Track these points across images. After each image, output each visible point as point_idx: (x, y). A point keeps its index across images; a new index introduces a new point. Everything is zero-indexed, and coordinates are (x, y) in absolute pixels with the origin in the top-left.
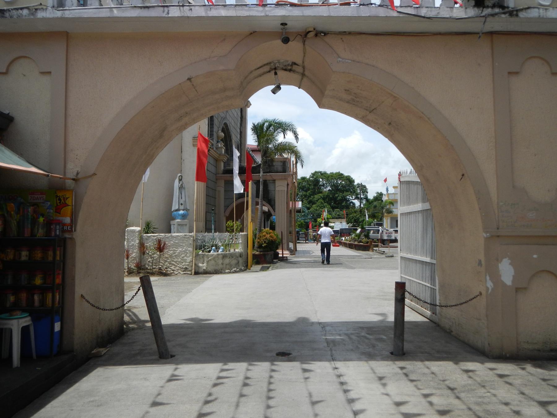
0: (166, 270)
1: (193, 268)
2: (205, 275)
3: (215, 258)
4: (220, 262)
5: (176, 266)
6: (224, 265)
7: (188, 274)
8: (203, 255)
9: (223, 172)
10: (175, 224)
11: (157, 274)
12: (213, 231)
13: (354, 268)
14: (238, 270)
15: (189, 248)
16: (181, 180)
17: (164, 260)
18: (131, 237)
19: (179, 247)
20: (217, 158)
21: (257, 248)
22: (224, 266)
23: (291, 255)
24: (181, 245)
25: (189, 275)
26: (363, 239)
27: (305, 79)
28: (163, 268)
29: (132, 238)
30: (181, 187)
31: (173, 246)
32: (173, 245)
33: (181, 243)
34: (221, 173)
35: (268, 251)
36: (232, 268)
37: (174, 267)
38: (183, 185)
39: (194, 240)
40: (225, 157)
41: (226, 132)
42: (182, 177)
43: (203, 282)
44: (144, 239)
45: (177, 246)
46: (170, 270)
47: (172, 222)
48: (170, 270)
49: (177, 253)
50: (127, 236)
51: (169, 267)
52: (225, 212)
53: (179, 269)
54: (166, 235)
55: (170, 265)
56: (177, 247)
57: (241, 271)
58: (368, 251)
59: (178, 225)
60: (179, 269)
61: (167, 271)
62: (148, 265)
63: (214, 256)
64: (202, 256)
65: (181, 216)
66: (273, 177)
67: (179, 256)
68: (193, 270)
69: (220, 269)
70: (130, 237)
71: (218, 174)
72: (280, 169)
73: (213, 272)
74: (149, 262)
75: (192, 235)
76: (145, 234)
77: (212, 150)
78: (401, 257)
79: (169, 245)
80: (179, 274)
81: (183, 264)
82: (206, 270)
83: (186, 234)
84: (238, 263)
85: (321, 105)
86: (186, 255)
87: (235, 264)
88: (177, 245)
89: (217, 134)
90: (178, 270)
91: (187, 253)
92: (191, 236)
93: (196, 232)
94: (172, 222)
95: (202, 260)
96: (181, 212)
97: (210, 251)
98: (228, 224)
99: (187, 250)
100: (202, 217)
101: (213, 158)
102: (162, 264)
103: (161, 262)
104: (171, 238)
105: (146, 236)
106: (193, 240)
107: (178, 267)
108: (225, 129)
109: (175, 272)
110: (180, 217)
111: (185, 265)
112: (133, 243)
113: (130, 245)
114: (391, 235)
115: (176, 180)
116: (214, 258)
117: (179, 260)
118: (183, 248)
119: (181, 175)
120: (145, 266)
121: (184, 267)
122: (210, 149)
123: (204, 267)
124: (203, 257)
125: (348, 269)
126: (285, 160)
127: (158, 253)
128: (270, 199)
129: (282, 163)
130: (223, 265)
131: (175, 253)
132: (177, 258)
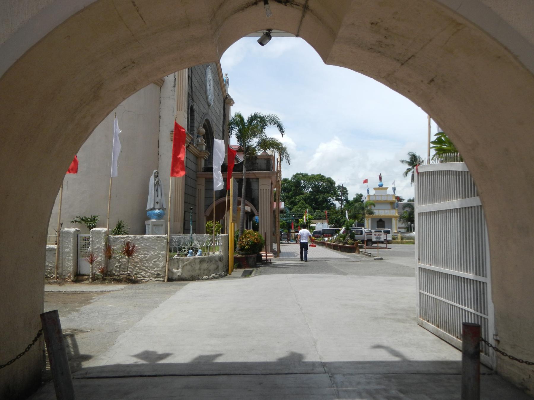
0: (135, 276)
1: (166, 274)
2: (179, 282)
3: (191, 263)
4: (197, 266)
5: (147, 272)
6: (202, 270)
7: (160, 281)
9: (204, 170)
10: (149, 225)
11: (125, 281)
12: (191, 232)
13: (345, 274)
14: (217, 275)
15: (162, 251)
16: (157, 176)
17: (134, 265)
18: (96, 239)
19: (150, 250)
20: (198, 156)
21: (238, 250)
22: (202, 271)
23: (274, 257)
24: (153, 248)
25: (161, 282)
26: (349, 240)
27: (308, 16)
28: (132, 274)
29: (97, 240)
30: (157, 184)
31: (143, 250)
32: (144, 248)
33: (153, 246)
34: (202, 170)
35: (250, 254)
36: (211, 273)
37: (144, 272)
38: (159, 181)
39: (168, 243)
40: (205, 154)
41: (208, 128)
42: (158, 173)
43: (176, 291)
44: (111, 241)
45: (148, 249)
46: (139, 276)
47: (147, 222)
48: (139, 276)
49: (148, 257)
50: (92, 237)
51: (139, 273)
52: (205, 212)
53: (151, 275)
54: (136, 237)
55: (141, 271)
56: (148, 250)
57: (221, 277)
58: (354, 252)
59: (153, 225)
60: (151, 275)
61: (137, 277)
62: (116, 271)
63: (190, 260)
64: (177, 260)
66: (257, 176)
67: (150, 261)
68: (166, 276)
69: (197, 275)
70: (95, 239)
71: (199, 172)
72: (264, 166)
73: (189, 279)
74: (117, 267)
75: (166, 237)
76: (113, 236)
77: (192, 146)
78: (419, 268)
79: (140, 248)
80: (150, 281)
81: (155, 270)
82: (180, 276)
83: (158, 235)
85: (326, 63)
86: (159, 259)
87: (214, 269)
88: (149, 248)
90: (149, 276)
91: (159, 257)
92: (164, 238)
93: (170, 233)
94: (147, 222)
95: (176, 265)
96: (157, 211)
97: (186, 255)
98: (208, 225)
99: (160, 254)
100: (180, 217)
101: (194, 154)
102: (131, 270)
103: (131, 268)
104: (141, 241)
105: (114, 238)
106: (166, 243)
107: (150, 273)
108: (207, 126)
109: (145, 278)
110: (155, 217)
111: (157, 271)
112: (98, 245)
113: (95, 247)
114: (380, 236)
115: (152, 177)
116: (190, 263)
117: (150, 265)
118: (155, 252)
119: (157, 172)
120: (112, 272)
121: (156, 273)
122: (190, 145)
123: (179, 273)
124: (178, 262)
125: (339, 274)
126: (269, 158)
127: (127, 257)
128: (253, 198)
129: (266, 161)
130: (200, 270)
131: (146, 257)
132: (148, 263)
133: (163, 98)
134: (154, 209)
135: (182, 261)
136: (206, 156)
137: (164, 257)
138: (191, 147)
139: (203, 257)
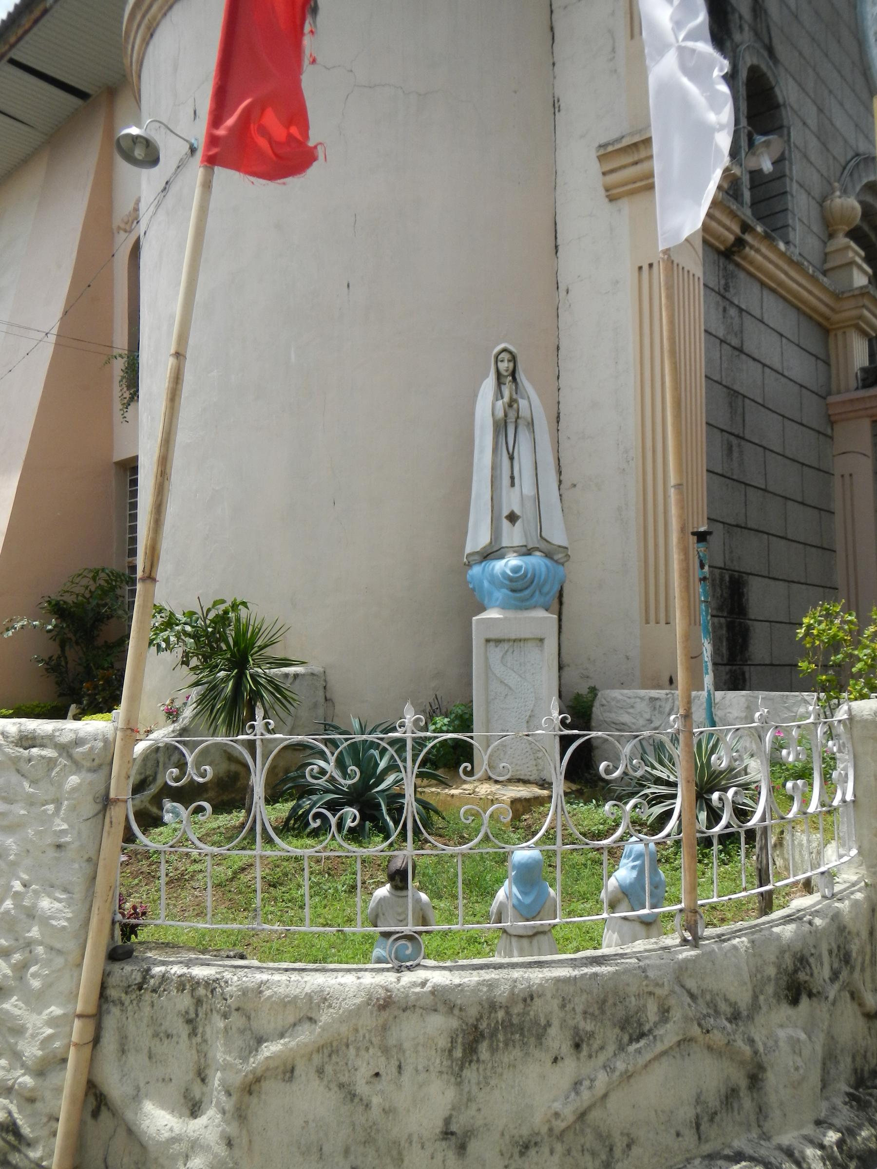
8: (199, 1002)
9: (863, 380)
15: (50, 887)
20: (828, 319)
34: (853, 384)
38: (523, 403)
40: (864, 306)
42: (513, 359)
59: (488, 641)
63: (324, 1018)
64: (185, 1001)
65: (502, 586)
71: (839, 392)
75: (78, 742)
84: (755, 1079)
87: (687, 1113)
89: (821, 204)
92: (65, 749)
101: (798, 309)
106: (89, 808)
110: (500, 595)
119: (505, 350)
122: (748, 237)
130: (462, 1148)
133: (565, 7)
134: (490, 554)
135: (237, 1021)
136: (866, 313)
137: (59, 952)
138: (752, 247)
139: (502, 993)
